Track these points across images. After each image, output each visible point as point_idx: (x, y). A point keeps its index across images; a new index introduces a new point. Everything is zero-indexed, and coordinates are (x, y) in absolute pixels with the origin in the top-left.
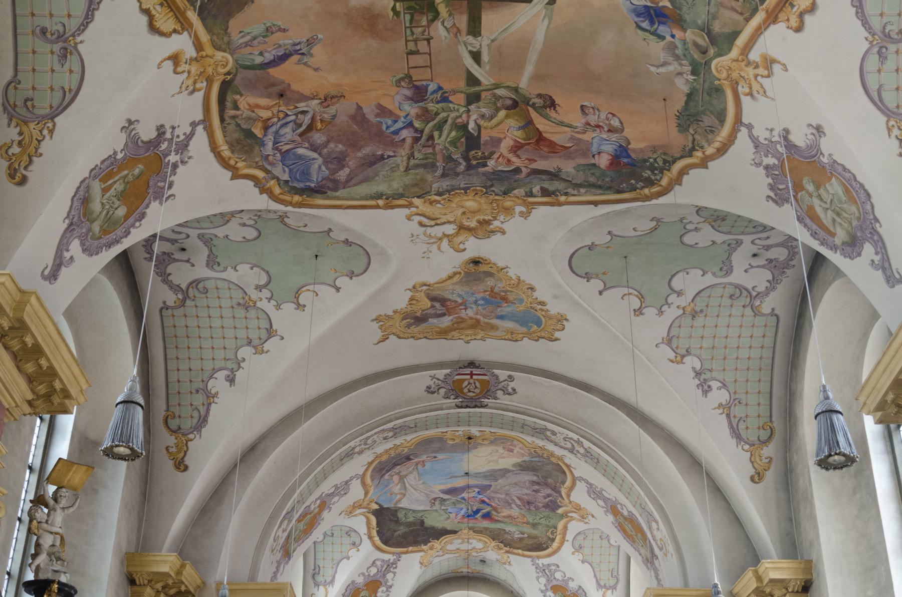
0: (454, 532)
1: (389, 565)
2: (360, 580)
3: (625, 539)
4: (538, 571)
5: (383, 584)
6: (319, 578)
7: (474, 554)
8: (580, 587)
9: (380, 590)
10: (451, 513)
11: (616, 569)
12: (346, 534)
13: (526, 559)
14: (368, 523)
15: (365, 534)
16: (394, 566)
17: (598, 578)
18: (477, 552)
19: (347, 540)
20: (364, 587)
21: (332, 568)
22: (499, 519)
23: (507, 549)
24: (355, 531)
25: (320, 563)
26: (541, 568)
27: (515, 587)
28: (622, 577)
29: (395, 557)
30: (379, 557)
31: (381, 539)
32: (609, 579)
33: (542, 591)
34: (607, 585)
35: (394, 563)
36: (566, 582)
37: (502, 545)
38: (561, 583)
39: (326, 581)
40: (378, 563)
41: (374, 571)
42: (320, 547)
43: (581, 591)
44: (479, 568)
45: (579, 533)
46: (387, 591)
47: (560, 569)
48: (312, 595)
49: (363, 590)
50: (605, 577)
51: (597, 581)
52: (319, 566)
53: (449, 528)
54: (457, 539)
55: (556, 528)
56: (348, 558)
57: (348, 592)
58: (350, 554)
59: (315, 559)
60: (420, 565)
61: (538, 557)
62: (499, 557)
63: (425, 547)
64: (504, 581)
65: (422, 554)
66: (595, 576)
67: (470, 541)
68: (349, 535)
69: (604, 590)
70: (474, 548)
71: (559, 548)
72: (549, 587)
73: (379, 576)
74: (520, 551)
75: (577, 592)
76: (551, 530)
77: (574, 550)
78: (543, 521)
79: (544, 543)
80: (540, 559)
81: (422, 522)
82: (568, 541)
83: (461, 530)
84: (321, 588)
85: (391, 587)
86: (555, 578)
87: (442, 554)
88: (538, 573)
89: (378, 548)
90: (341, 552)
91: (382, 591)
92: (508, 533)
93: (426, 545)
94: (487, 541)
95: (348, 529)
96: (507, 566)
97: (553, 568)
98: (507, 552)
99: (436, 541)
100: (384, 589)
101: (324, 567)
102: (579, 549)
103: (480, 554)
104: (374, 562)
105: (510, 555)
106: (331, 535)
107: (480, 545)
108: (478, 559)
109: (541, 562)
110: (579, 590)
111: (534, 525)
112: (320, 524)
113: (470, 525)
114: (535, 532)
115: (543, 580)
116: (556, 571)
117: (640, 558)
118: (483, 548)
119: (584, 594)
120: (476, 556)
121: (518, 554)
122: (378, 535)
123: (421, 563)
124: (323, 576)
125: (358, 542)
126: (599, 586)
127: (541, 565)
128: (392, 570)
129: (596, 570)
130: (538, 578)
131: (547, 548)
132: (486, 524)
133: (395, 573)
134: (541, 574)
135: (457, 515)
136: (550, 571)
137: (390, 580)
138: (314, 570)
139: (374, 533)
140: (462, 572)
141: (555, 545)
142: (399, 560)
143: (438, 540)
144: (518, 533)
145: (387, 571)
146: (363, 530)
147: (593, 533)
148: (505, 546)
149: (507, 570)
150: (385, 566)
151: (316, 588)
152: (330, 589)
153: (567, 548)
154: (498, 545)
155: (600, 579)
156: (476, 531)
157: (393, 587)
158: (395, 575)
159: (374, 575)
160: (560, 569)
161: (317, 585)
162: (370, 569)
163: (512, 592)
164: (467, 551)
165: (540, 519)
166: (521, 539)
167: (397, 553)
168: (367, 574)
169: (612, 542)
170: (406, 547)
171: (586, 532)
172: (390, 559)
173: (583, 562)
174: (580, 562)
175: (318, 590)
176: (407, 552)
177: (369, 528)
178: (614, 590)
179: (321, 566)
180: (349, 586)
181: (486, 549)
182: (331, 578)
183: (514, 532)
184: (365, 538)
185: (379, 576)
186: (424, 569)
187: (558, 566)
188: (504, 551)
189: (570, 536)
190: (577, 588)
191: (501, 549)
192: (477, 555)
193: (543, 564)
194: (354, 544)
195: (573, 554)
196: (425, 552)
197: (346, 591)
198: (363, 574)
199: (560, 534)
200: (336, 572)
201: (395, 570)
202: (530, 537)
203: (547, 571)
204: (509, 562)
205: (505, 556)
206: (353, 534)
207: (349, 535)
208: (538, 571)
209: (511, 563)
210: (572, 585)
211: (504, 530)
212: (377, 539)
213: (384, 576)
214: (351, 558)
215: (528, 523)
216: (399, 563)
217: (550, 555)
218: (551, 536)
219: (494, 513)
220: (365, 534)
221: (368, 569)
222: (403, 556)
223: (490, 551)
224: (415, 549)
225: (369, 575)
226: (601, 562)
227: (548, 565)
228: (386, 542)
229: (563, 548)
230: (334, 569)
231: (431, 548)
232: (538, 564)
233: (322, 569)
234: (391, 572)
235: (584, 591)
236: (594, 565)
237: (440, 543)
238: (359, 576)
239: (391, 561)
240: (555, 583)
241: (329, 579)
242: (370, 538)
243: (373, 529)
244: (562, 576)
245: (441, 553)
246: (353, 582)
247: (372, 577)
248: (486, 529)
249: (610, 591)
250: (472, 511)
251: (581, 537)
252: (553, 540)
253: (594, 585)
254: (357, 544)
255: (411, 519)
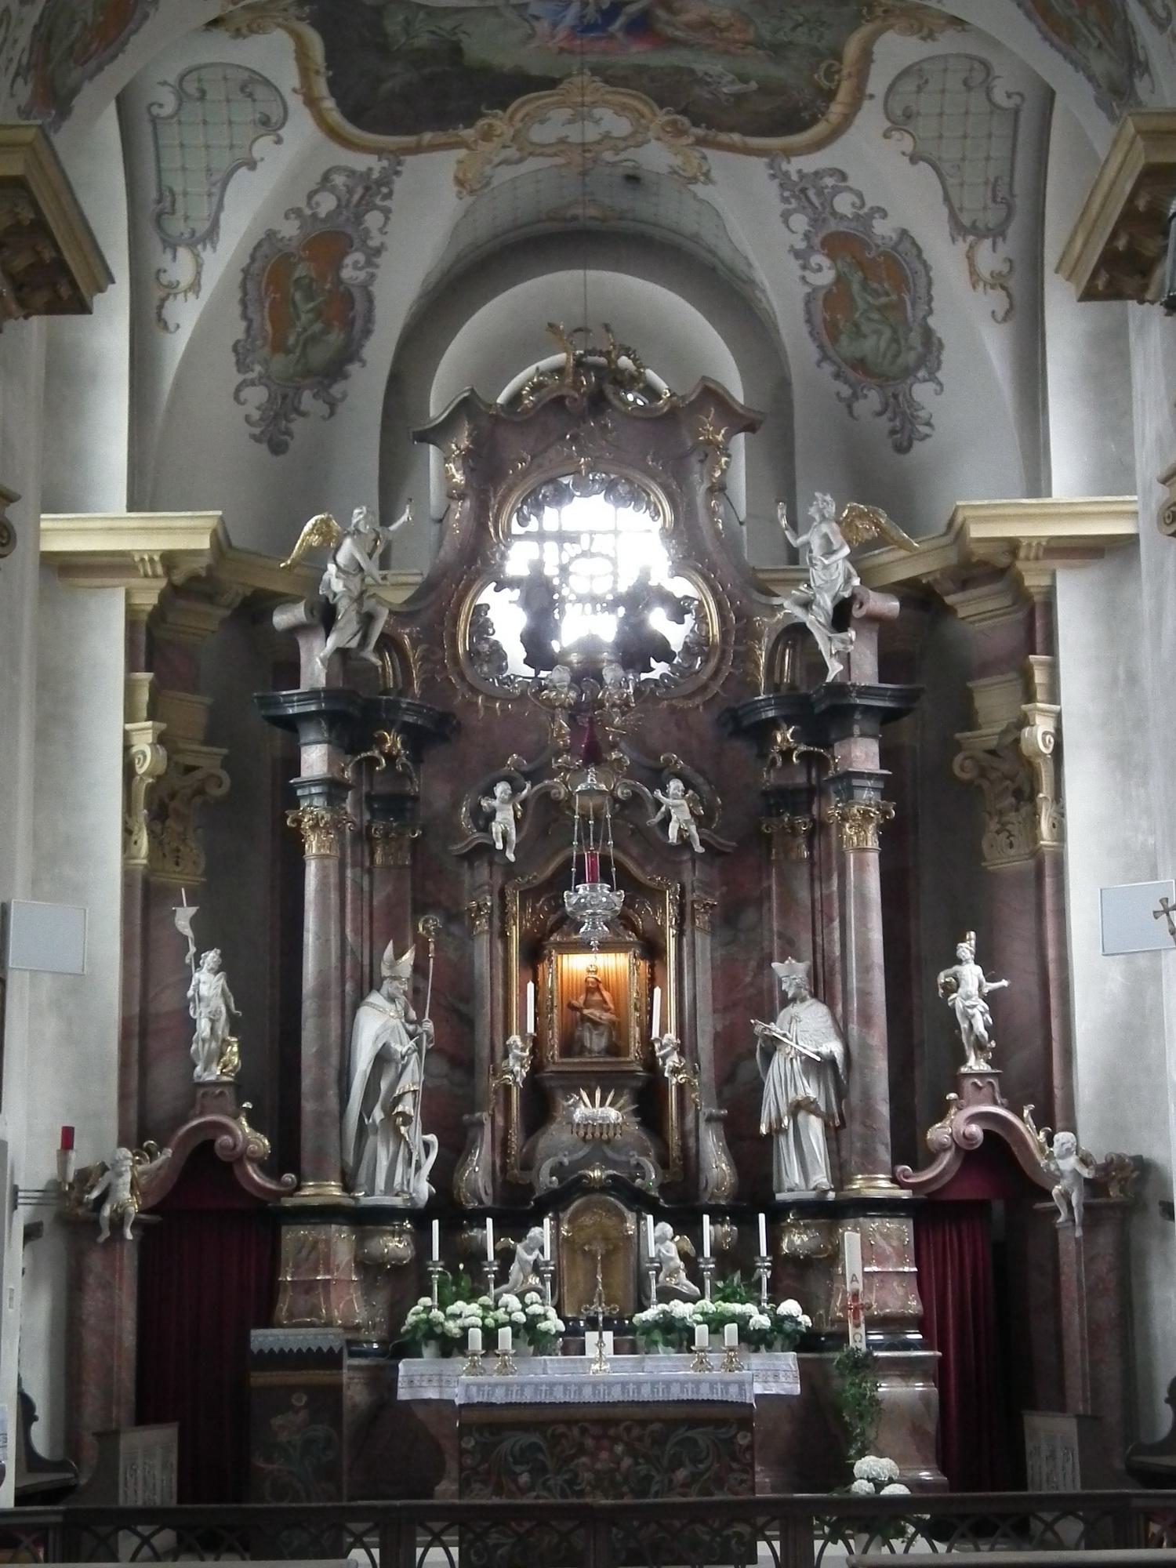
0: (549, 83)
1: (367, 189)
2: (290, 230)
3: (1046, 38)
4: (787, 194)
5: (357, 243)
6: (177, 226)
7: (608, 156)
8: (904, 233)
9: (349, 260)
10: (537, 18)
11: (1007, 179)
12: (242, 89)
13: (754, 159)
14: (302, 54)
15: (295, 91)
16: (385, 190)
17: (956, 206)
18: (617, 151)
19: (245, 112)
20: (304, 250)
21: (210, 195)
22: (679, 34)
23: (700, 132)
24: (267, 82)
25: (176, 182)
26: (795, 184)
27: (724, 251)
28: (1021, 203)
29: (385, 163)
30: (343, 163)
31: (341, 104)
32: (985, 208)
33: (797, 254)
34: (980, 225)
35: (385, 181)
36: (865, 220)
37: (685, 121)
38: (853, 224)
39: (193, 233)
40: (339, 180)
41: (327, 203)
42: (170, 135)
43: (907, 244)
44: (625, 200)
45: (905, 73)
46: (369, 263)
47: (850, 183)
48: (159, 271)
49: (301, 259)
50: (975, 203)
51: (953, 217)
52: (173, 194)
53: (535, 71)
54: (561, 105)
55: (838, 56)
56: (252, 165)
57: (257, 265)
58: (256, 154)
59: (159, 171)
60: (456, 189)
61: (789, 153)
62: (677, 161)
63: (468, 134)
64: (695, 238)
65: (462, 153)
66: (947, 199)
67: (598, 112)
68: (250, 95)
69: (971, 238)
70: (607, 136)
71: (847, 121)
72: (817, 241)
73: (342, 218)
74: (736, 137)
75: (894, 248)
76: (824, 66)
77: (888, 124)
78: (801, 37)
79: (806, 108)
80: (794, 160)
81: (456, 50)
82: (872, 96)
83: (569, 75)
84: (183, 253)
85: (378, 251)
86: (834, 213)
87: (517, 155)
88: (785, 200)
89: (333, 133)
90: (232, 147)
91: (356, 266)
92: (700, 81)
93: (469, 124)
94: (646, 111)
95: (246, 75)
96: (699, 189)
97: (829, 181)
98: (701, 142)
99: (500, 112)
100: (358, 257)
101: (185, 194)
102: (901, 121)
103: (623, 156)
104: (326, 177)
105: (709, 152)
106: (197, 95)
107: (621, 126)
108: (620, 171)
109: (795, 166)
110: (900, 240)
111: (777, 51)
112: (146, 16)
113: (592, 59)
114: (778, 73)
115: (800, 222)
116: (837, 191)
117: (1089, 90)
118: (634, 134)
119: (914, 252)
120: (614, 164)
121: (731, 148)
122: (333, 93)
123: (460, 182)
124: (186, 218)
125: (276, 116)
126: (959, 228)
127: (795, 177)
128: (378, 201)
129: (950, 181)
130: (786, 216)
131: (814, 121)
132: (638, 53)
133: (387, 212)
134: (794, 204)
135: (554, 25)
136: (820, 193)
137: (374, 233)
138: (159, 201)
139: (321, 87)
140: (575, 218)
141: (836, 110)
142: (397, 173)
143: (504, 108)
144: (731, 77)
145: (366, 204)
146: (288, 78)
147: (945, 70)
148: (696, 124)
149: (702, 201)
150: (360, 191)
151: (169, 255)
152: (207, 255)
153: (871, 119)
154: (674, 123)
155: (961, 209)
156: (612, 78)
157: (384, 254)
158: (387, 219)
159: (329, 215)
160: (850, 183)
161: (171, 244)
162: (317, 198)
163: (714, 269)
164: (584, 147)
165: (794, 29)
166: (740, 98)
167: (391, 152)
168: (308, 212)
169: (999, 97)
170: (409, 132)
171: (926, 66)
172: (370, 170)
173: (914, 159)
174: (906, 159)
175: (174, 258)
176: (417, 150)
177: (305, 72)
178: (1000, 240)
179: (178, 189)
180: (259, 246)
181: (636, 140)
182: (207, 225)
183: (720, 76)
184: (295, 103)
185: (342, 218)
186: (469, 199)
187: (843, 176)
188: (691, 140)
189: (877, 84)
190: (895, 237)
191: (680, 133)
192: (617, 158)
193: (800, 171)
194: (265, 122)
195: (886, 135)
196: (468, 147)
197: (253, 258)
198: (298, 212)
199: (850, 75)
200: (220, 207)
201: (387, 203)
202: (765, 90)
203: (811, 193)
204: (707, 175)
205: (695, 154)
206: (260, 92)
207: (250, 95)
208: (787, 194)
209: (714, 174)
210: (883, 229)
211: (692, 72)
212: (329, 104)
213: (358, 219)
214: (260, 165)
215: (758, 44)
216: (398, 184)
217: (819, 145)
218: (825, 84)
219: (661, 13)
220: (295, 91)
221: (311, 195)
222: (410, 160)
223: (653, 142)
224: (442, 137)
225: (314, 216)
226: (963, 159)
227: (816, 173)
228: (354, 115)
229: (860, 120)
230: (215, 199)
231: (487, 136)
232: (786, 174)
233: (180, 200)
234: (376, 207)
235: (914, 243)
236: (946, 168)
237: (511, 118)
238: (287, 217)
239: (375, 175)
240: (833, 226)
241: (202, 227)
242: (311, 102)
243: (318, 72)
244: (853, 205)
245: (512, 152)
246: (271, 235)
247: (324, 221)
248: (641, 70)
249: (987, 243)
250: (600, 10)
251: (909, 86)
252: (830, 95)
253: (944, 227)
254: (274, 119)
255: (423, 41)
